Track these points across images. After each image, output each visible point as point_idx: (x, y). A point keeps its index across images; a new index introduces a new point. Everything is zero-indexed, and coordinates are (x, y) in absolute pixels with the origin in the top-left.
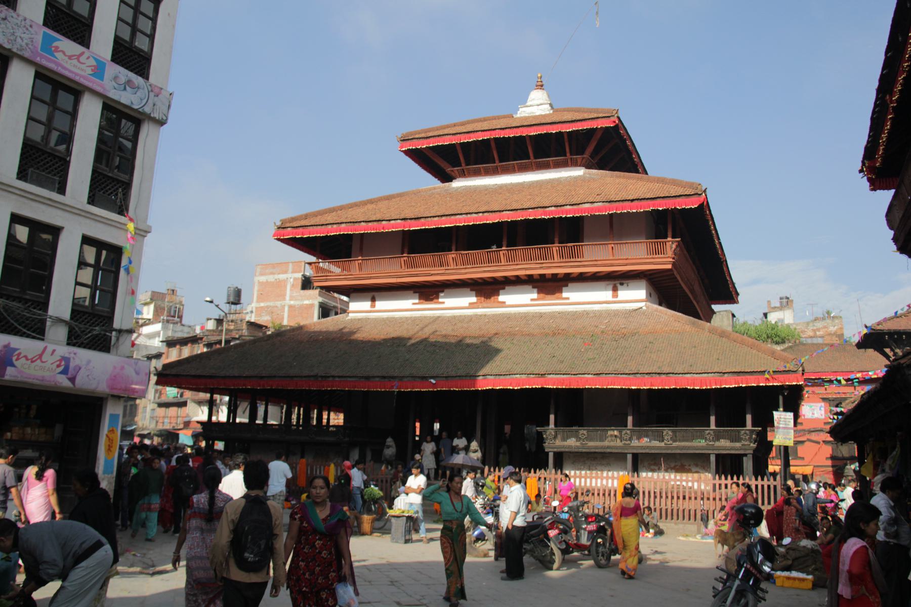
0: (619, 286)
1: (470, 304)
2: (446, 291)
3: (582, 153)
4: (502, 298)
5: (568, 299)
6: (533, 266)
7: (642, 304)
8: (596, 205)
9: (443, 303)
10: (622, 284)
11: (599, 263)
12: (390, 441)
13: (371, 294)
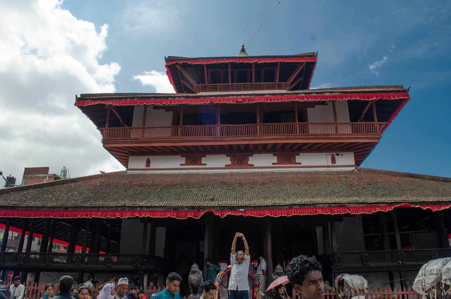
0: (335, 155)
1: (226, 165)
3: (286, 82)
4: (252, 160)
5: (300, 163)
6: (281, 137)
8: (334, 94)
9: (205, 164)
10: (338, 155)
11: (330, 136)
12: (195, 267)
13: (147, 157)
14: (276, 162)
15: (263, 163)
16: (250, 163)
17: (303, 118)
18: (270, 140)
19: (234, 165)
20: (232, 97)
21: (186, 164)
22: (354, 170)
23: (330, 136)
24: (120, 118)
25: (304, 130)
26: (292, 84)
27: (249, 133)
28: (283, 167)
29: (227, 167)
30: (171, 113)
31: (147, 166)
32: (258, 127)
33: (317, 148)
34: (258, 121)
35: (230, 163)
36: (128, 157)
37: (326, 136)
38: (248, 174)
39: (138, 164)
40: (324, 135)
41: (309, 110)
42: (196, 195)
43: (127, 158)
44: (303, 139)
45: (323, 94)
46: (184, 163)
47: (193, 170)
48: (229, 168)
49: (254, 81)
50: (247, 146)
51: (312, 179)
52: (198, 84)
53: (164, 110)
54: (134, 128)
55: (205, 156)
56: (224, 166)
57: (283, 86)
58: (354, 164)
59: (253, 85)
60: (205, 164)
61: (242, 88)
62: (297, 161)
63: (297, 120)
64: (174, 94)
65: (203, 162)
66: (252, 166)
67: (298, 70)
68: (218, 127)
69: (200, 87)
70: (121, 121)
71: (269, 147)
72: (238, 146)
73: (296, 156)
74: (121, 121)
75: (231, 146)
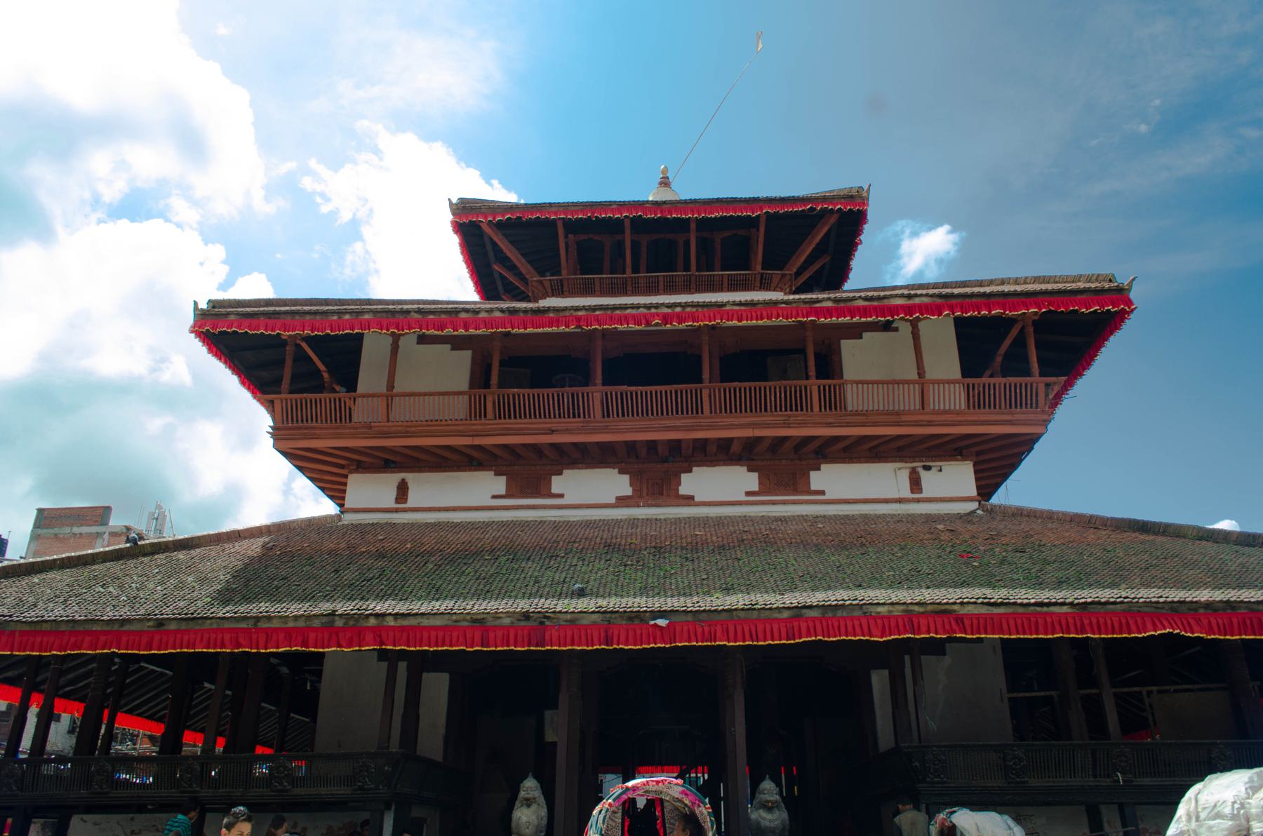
1: (618, 498)
5: (823, 493)
7: (974, 505)
9: (561, 496)
10: (928, 468)
12: (530, 786)
14: (756, 488)
15: (719, 489)
16: (684, 490)
17: (829, 365)
18: (739, 429)
19: (641, 497)
20: (634, 311)
21: (508, 496)
22: (974, 512)
23: (904, 418)
24: (322, 367)
25: (832, 401)
26: (798, 274)
27: (680, 410)
28: (774, 503)
30: (467, 354)
31: (398, 500)
32: (705, 393)
33: (870, 449)
34: (706, 375)
35: (628, 491)
36: (346, 477)
37: (895, 417)
38: (677, 521)
39: (371, 493)
40: (888, 413)
41: (847, 346)
42: (536, 582)
43: (343, 480)
44: (829, 425)
45: (886, 302)
46: (503, 492)
47: (529, 511)
48: (628, 506)
49: (693, 267)
50: (675, 446)
51: (858, 540)
52: (542, 274)
53: (449, 346)
54: (363, 396)
55: (560, 474)
56: (613, 501)
57: (775, 280)
58: (974, 492)
59: (693, 279)
60: (561, 496)
61: (661, 286)
62: (814, 486)
63: (812, 372)
64: (475, 303)
65: (554, 490)
66: (689, 500)
67: (819, 235)
68: (597, 393)
69: (547, 284)
70: (326, 375)
71: (736, 448)
72: (652, 445)
73: (813, 474)
74: (326, 375)
75: (631, 447)
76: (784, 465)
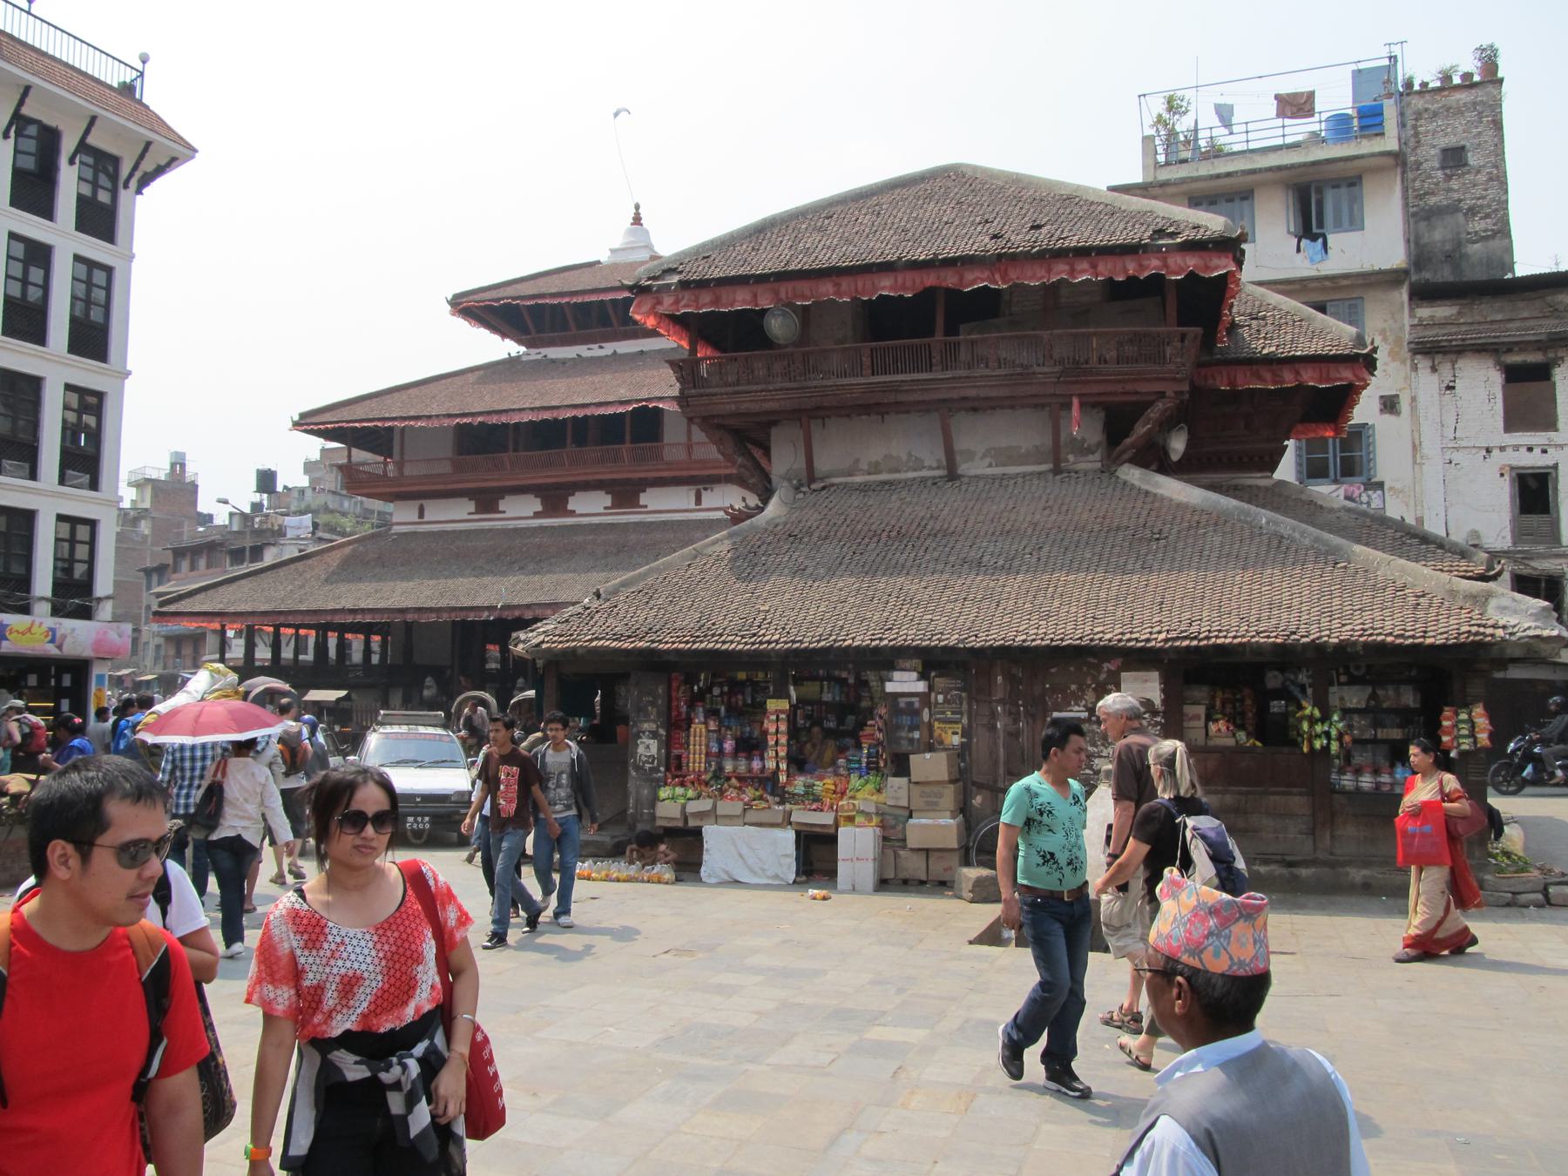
2: (507, 498)
16: (570, 507)
29: (537, 515)
34: (569, 440)
35: (539, 508)
63: (628, 437)
66: (572, 513)
76: (626, 494)
